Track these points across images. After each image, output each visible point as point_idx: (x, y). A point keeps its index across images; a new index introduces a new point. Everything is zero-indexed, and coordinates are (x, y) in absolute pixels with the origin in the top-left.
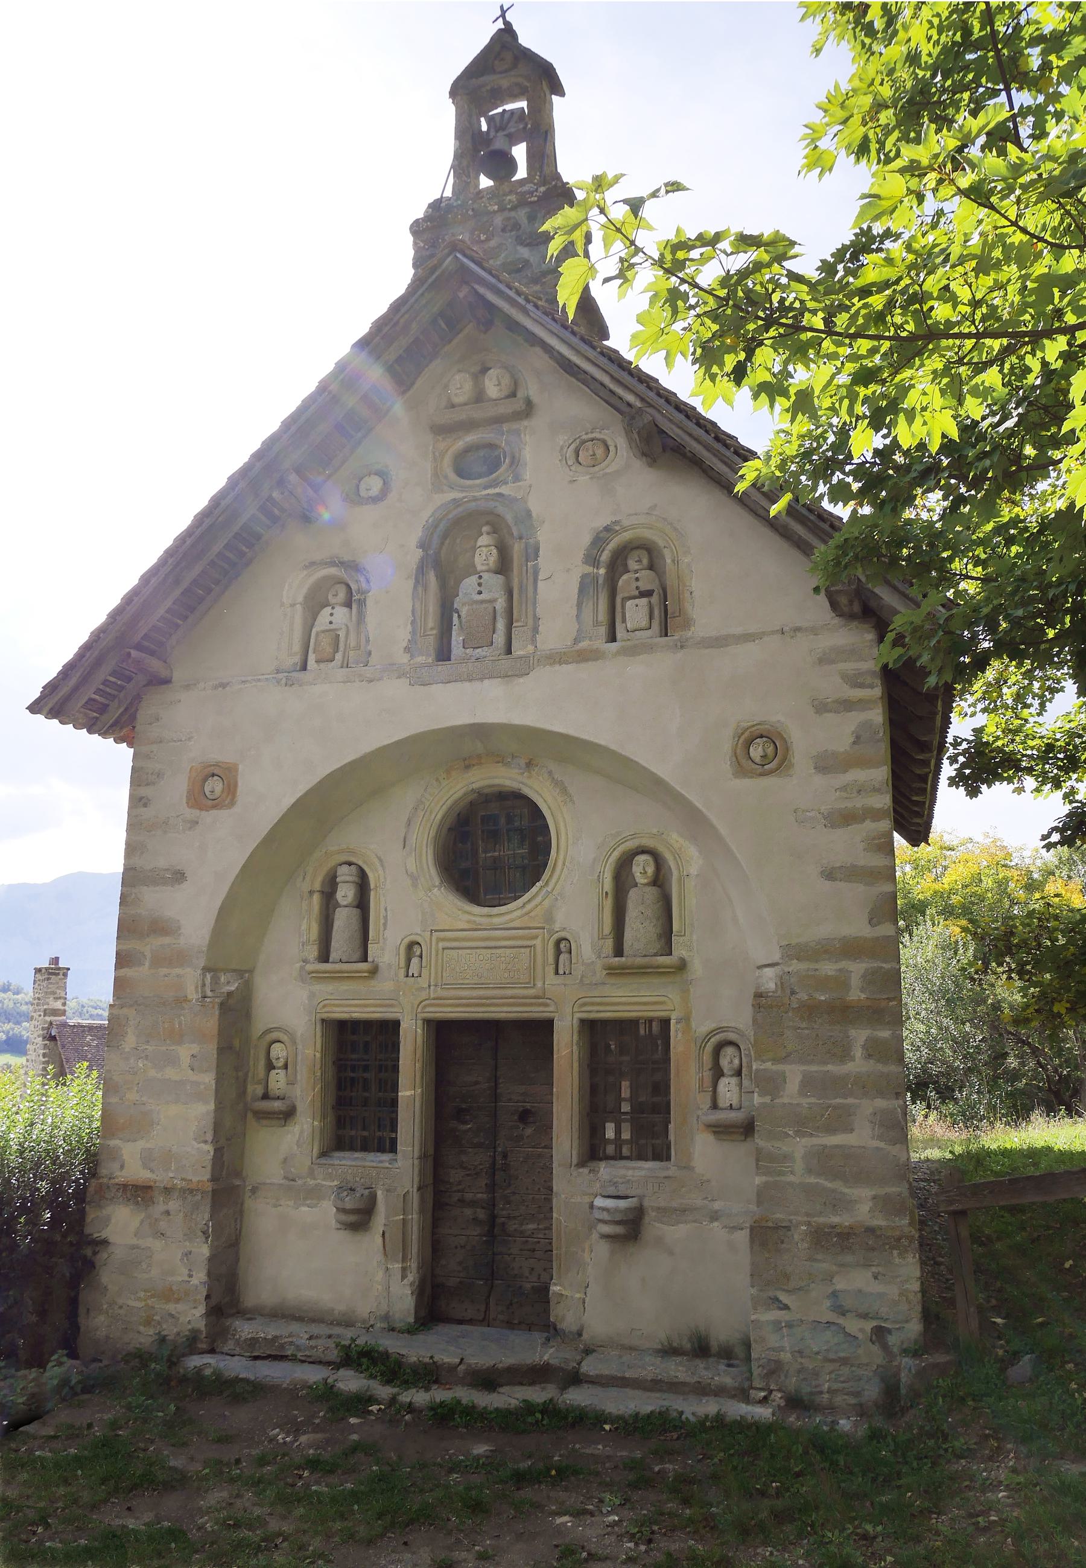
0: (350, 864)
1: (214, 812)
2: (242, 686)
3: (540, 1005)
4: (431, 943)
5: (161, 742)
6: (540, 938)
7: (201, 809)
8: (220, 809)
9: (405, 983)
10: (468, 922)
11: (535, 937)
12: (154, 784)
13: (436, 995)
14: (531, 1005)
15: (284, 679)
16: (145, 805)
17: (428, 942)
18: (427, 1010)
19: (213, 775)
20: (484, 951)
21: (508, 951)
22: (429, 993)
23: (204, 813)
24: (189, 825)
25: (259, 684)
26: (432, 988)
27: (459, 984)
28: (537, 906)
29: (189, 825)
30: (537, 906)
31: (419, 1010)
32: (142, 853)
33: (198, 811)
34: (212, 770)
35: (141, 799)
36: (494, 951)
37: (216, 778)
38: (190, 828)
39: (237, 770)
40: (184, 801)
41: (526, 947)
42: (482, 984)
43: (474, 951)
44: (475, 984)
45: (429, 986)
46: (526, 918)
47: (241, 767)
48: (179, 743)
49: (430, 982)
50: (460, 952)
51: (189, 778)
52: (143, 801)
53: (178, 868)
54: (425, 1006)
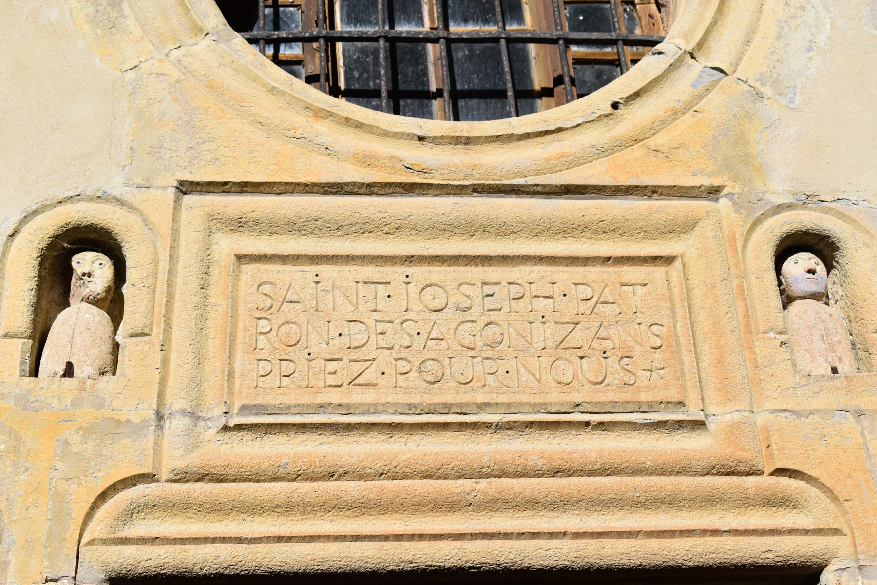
3: (746, 502)
4: (175, 233)
6: (705, 229)
9: (24, 402)
10: (365, 160)
11: (687, 227)
13: (195, 460)
14: (710, 501)
17: (165, 229)
18: (141, 528)
20: (437, 272)
21: (565, 274)
22: (157, 446)
26: (176, 425)
27: (322, 407)
28: (675, 114)
30: (675, 114)
31: (95, 529)
36: (493, 273)
41: (655, 260)
42: (447, 408)
43: (396, 273)
44: (411, 408)
45: (160, 417)
46: (637, 151)
49: (161, 396)
50: (327, 271)
54: (132, 512)
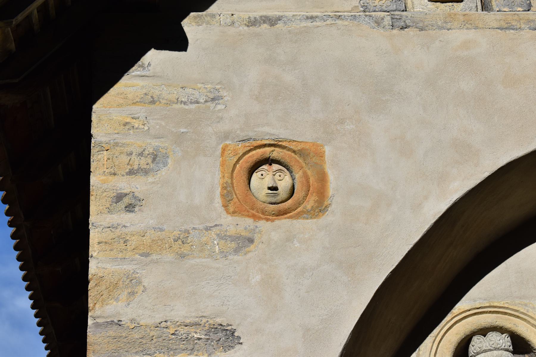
0: (501, 330)
1: (284, 222)
2: (309, 24)
5: (153, 102)
7: (254, 217)
8: (298, 216)
12: (147, 172)
15: (389, 18)
16: (130, 208)
19: (268, 161)
23: (263, 224)
24: (233, 245)
25: (339, 22)
29: (233, 245)
32: (132, 294)
33: (249, 221)
34: (276, 153)
35: (119, 197)
37: (275, 167)
38: (236, 251)
39: (321, 155)
40: (218, 202)
47: (328, 150)
48: (193, 106)
51: (223, 164)
52: (126, 201)
53: (219, 320)
